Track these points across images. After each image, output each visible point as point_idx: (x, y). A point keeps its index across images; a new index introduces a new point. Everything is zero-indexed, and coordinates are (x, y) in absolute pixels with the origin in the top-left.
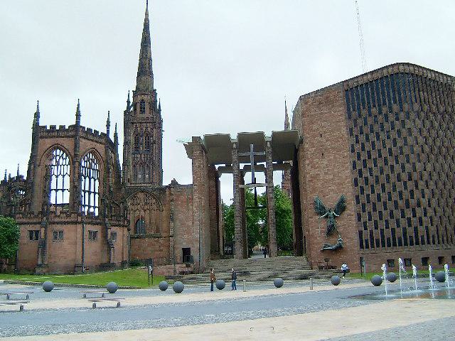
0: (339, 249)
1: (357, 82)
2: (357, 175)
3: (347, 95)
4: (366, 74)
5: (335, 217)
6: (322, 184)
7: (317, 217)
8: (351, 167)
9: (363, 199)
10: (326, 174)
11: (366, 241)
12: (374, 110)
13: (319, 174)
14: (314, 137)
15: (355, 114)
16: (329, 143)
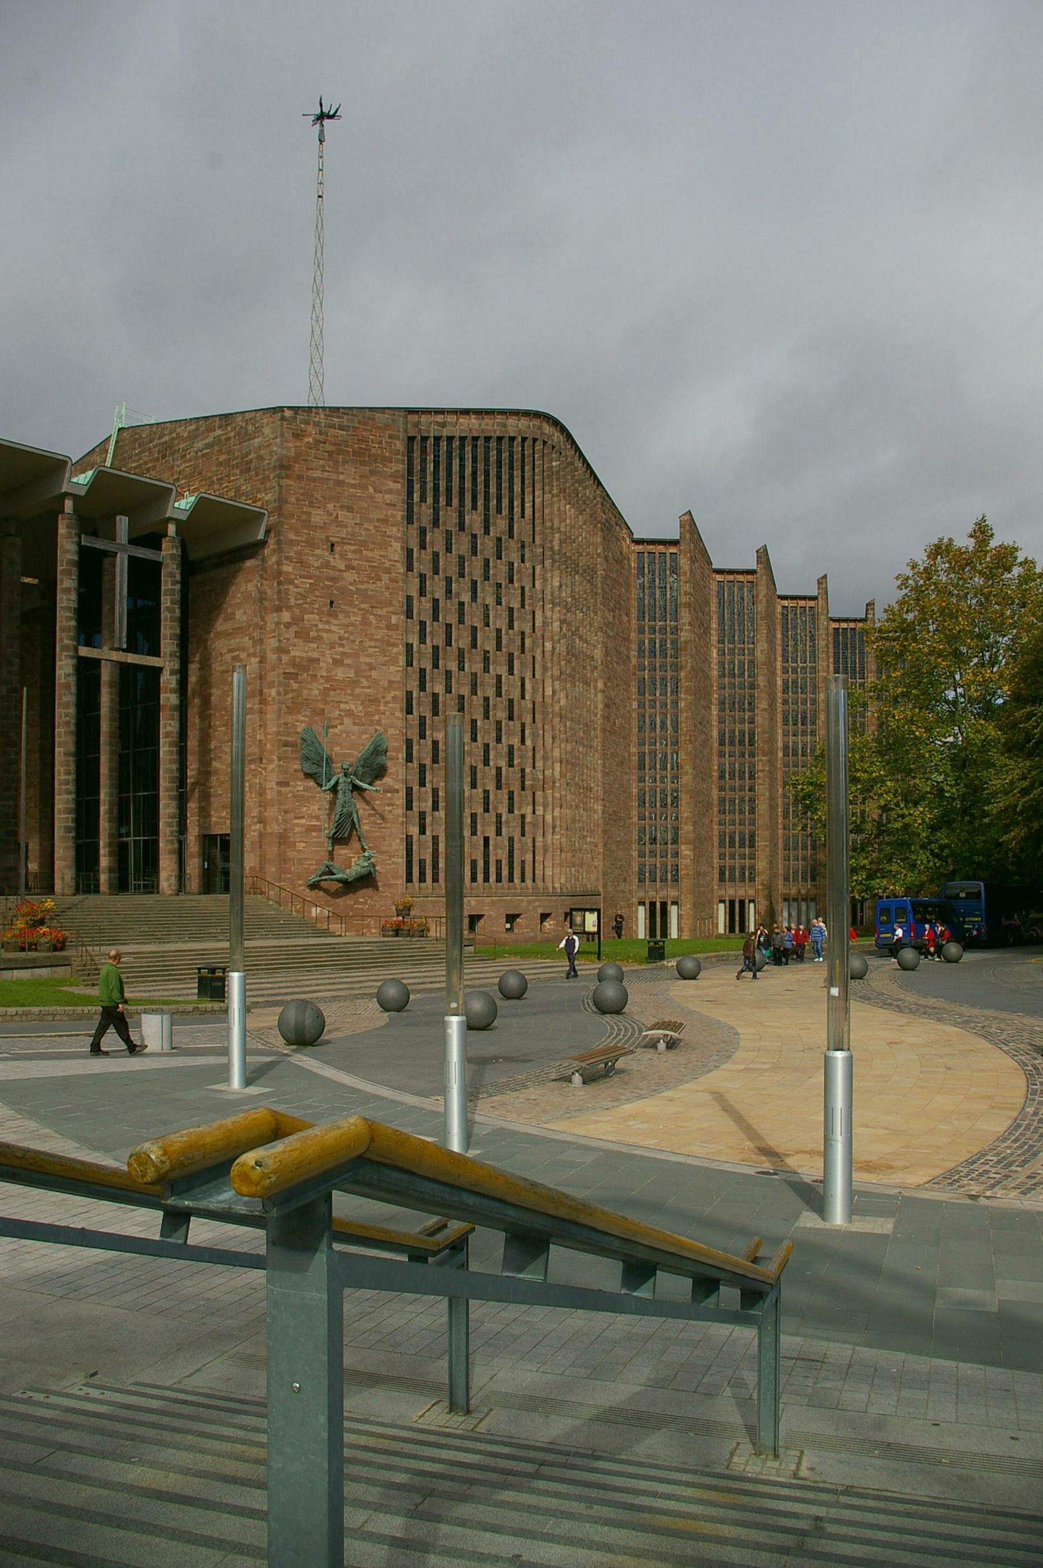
0: (366, 880)
1: (443, 425)
2: (414, 685)
3: (410, 450)
4: (466, 412)
5: (356, 788)
6: (325, 692)
7: (301, 785)
8: (402, 661)
9: (423, 751)
10: (336, 662)
11: (422, 863)
12: (474, 520)
13: (318, 660)
14: (312, 544)
15: (424, 512)
16: (350, 576)
